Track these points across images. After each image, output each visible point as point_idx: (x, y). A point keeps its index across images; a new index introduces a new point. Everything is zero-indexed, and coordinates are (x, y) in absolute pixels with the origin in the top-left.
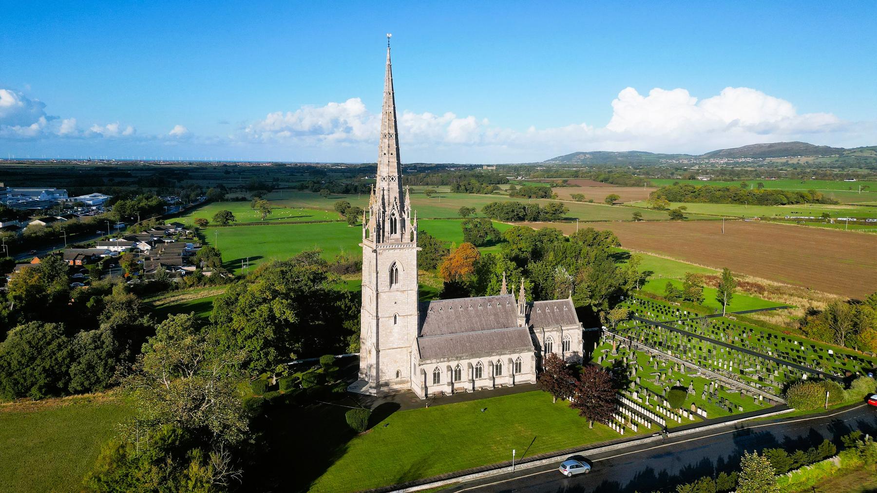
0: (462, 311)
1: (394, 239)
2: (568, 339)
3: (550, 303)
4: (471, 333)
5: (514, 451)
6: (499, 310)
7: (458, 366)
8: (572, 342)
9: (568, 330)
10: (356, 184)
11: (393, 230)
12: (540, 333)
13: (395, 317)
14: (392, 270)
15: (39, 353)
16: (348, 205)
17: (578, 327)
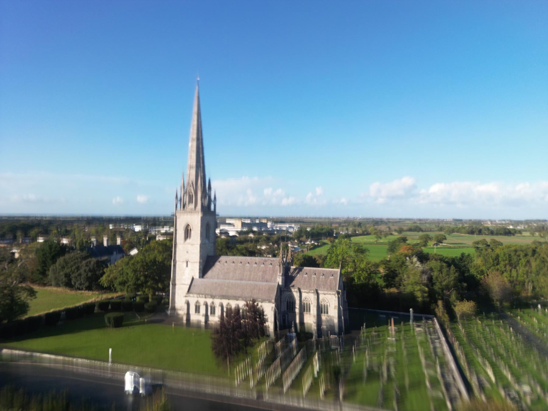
0: (240, 266)
1: (189, 209)
2: (326, 303)
3: (319, 271)
4: (239, 282)
5: (110, 350)
6: (268, 269)
7: (213, 303)
8: (330, 305)
9: (325, 294)
10: (481, 228)
11: (190, 201)
12: (297, 292)
13: (187, 262)
14: (188, 230)
15: (66, 265)
16: (444, 237)
17: (334, 293)
